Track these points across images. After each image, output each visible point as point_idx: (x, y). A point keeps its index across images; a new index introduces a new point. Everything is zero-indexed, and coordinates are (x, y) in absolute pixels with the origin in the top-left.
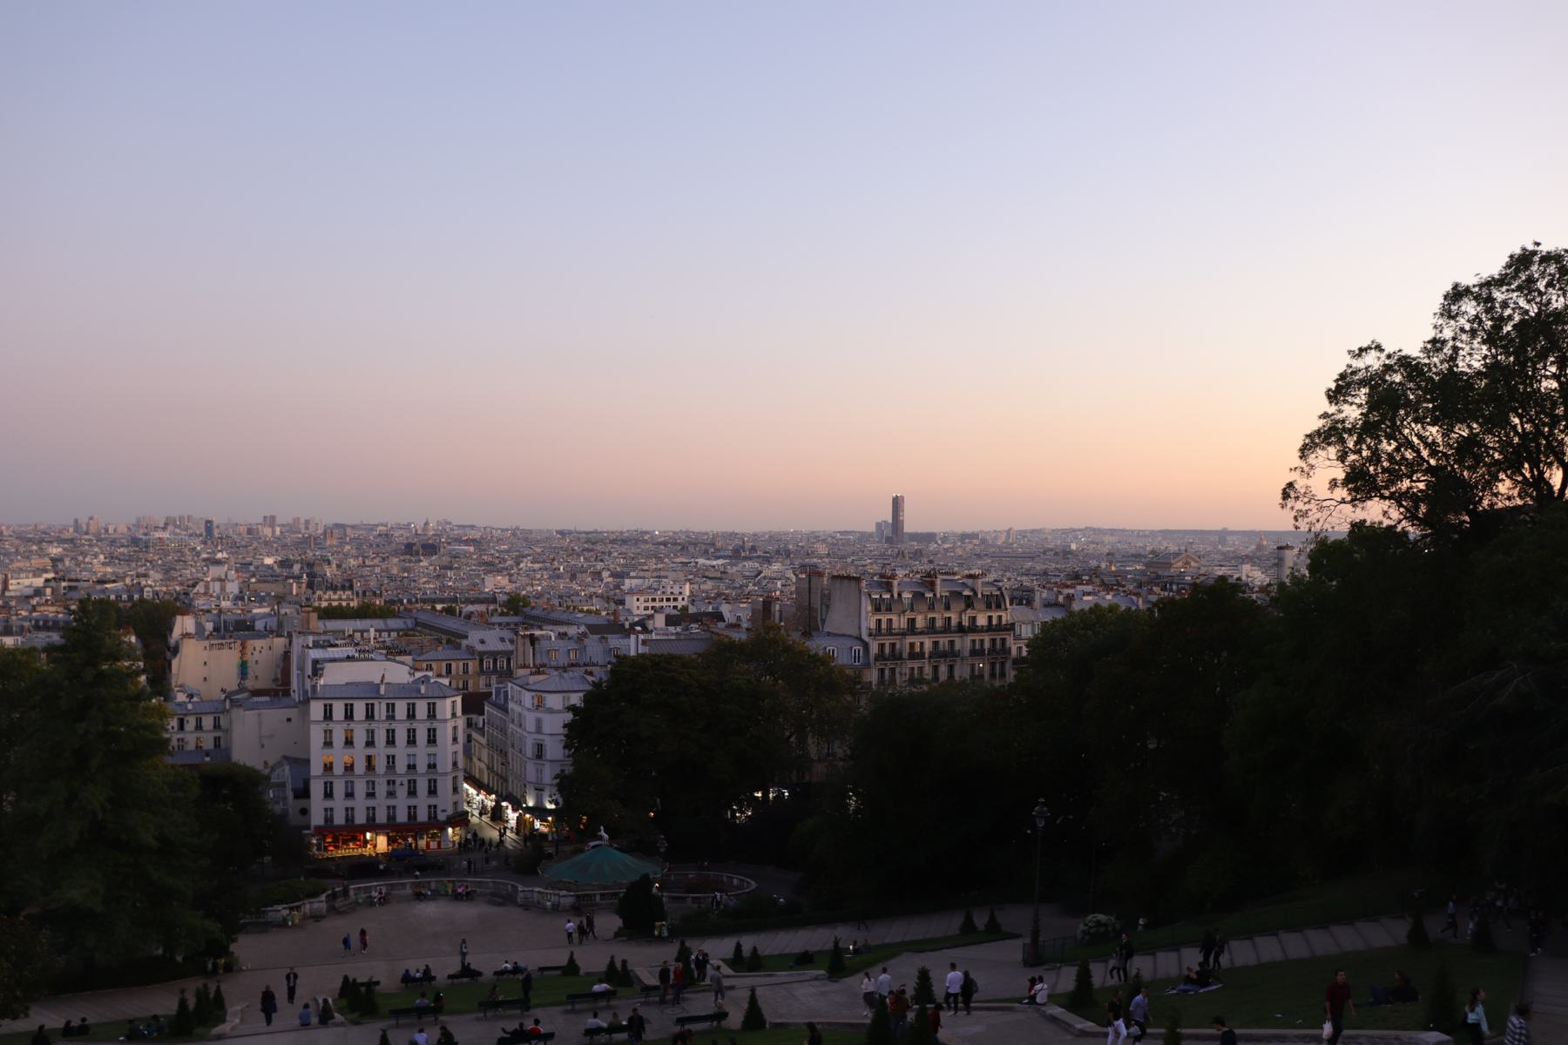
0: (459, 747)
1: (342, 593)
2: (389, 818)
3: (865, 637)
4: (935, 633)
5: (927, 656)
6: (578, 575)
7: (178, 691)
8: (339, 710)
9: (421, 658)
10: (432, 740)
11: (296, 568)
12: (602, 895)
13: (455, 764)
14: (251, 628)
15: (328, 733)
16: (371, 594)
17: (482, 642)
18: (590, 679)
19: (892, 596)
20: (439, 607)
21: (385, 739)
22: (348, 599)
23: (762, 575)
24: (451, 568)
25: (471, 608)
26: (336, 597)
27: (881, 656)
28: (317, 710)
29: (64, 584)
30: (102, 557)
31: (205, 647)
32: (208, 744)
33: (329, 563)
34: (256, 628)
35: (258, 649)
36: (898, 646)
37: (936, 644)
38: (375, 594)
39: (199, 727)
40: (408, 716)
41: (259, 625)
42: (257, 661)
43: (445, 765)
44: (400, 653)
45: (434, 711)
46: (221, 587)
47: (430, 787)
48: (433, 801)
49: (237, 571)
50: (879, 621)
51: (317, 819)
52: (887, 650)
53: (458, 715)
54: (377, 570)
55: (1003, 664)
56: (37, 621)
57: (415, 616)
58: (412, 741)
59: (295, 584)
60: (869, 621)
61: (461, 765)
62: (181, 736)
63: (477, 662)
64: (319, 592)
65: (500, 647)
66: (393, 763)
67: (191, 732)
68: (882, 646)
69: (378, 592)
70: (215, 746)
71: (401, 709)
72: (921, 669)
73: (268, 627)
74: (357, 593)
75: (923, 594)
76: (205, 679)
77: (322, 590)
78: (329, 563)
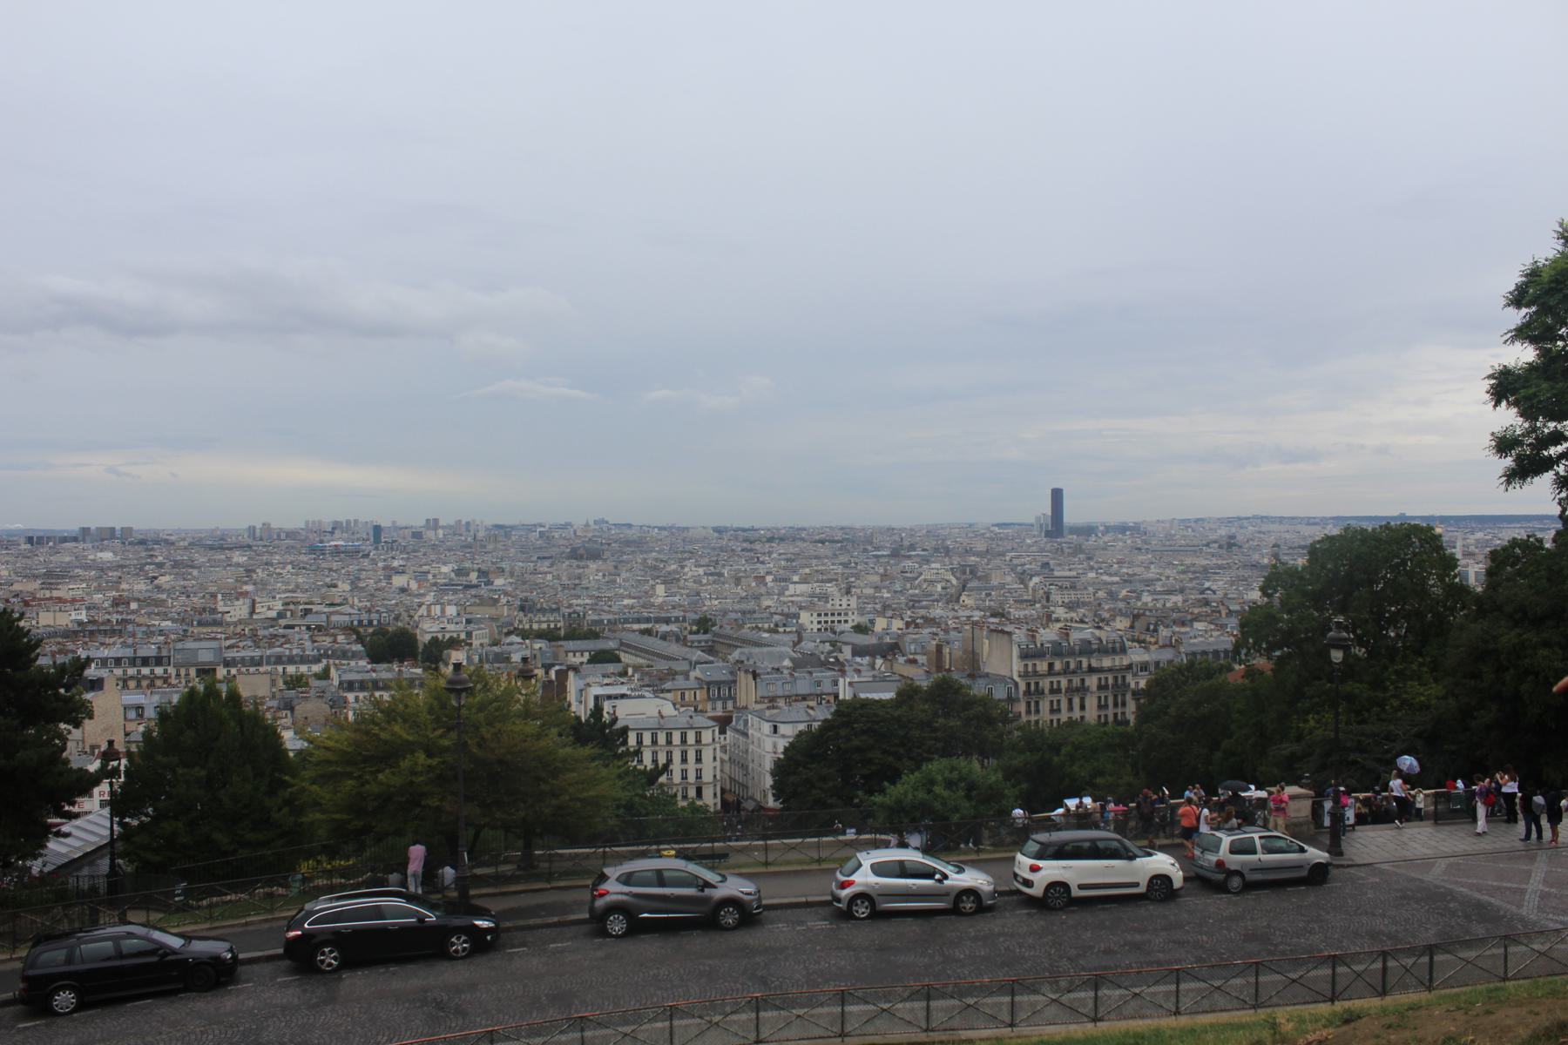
0: (718, 763)
3: (1016, 678)
4: (1070, 673)
5: (1063, 691)
6: (743, 580)
10: (699, 760)
13: (715, 776)
18: (811, 712)
20: (636, 627)
22: (556, 621)
23: (922, 577)
24: (619, 575)
26: (545, 619)
27: (1028, 692)
29: (301, 607)
30: (289, 567)
34: (513, 660)
36: (1041, 684)
37: (1070, 681)
38: (579, 615)
43: (707, 777)
49: (419, 581)
52: (1033, 688)
53: (717, 739)
54: (549, 577)
55: (1124, 695)
58: (684, 760)
60: (1017, 666)
61: (718, 777)
68: (1028, 685)
71: (676, 738)
72: (1059, 701)
78: (503, 571)
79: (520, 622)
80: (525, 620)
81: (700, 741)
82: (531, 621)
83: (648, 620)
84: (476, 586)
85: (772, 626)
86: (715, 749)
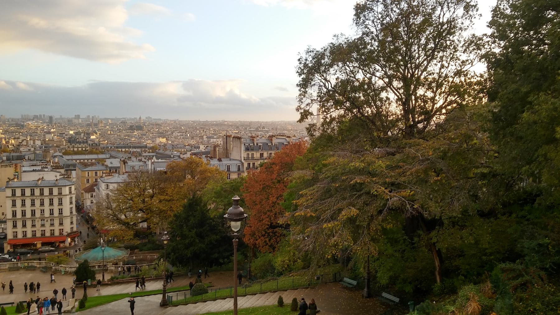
0: (74, 206)
2: (42, 235)
3: (243, 161)
8: (18, 192)
11: (82, 135)
12: (98, 266)
13: (71, 213)
16: (95, 145)
17: (111, 163)
19: (254, 144)
20: (123, 150)
21: (58, 202)
22: (86, 147)
25: (135, 150)
26: (80, 146)
28: (9, 192)
33: (96, 133)
36: (256, 164)
38: (97, 145)
40: (50, 194)
41: (27, 157)
43: (66, 212)
45: (52, 192)
46: (33, 142)
47: (60, 222)
48: (61, 228)
50: (249, 154)
51: (10, 236)
52: (251, 166)
53: (73, 192)
58: (51, 204)
60: (244, 154)
65: (119, 165)
66: (44, 212)
68: (249, 164)
69: (98, 144)
71: (46, 192)
74: (89, 144)
75: (267, 144)
78: (96, 133)
79: (69, 147)
80: (70, 146)
81: (61, 193)
82: (73, 147)
83: (130, 147)
85: (185, 150)
86: (71, 198)
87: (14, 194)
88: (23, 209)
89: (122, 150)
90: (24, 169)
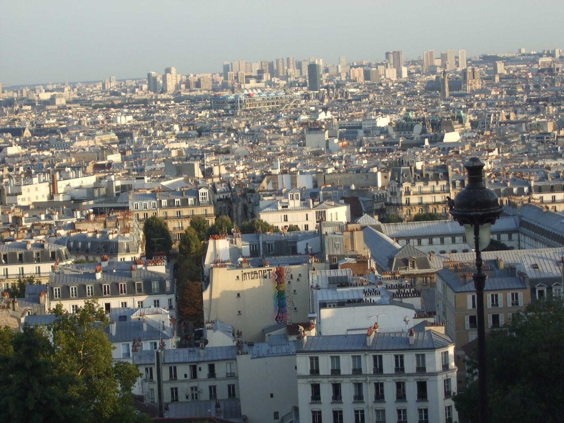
1: (434, 183)
7: (208, 329)
9: (463, 289)
11: (418, 128)
14: (294, 251)
15: (316, 389)
17: (535, 267)
26: (427, 189)
30: (176, 127)
31: (238, 277)
32: (222, 393)
33: (461, 121)
35: (295, 277)
39: (212, 373)
40: (397, 369)
41: (301, 246)
42: (295, 291)
44: (406, 295)
56: (76, 243)
57: (519, 213)
59: (379, 174)
62: (194, 384)
63: (528, 291)
64: (406, 185)
67: (204, 380)
70: (230, 395)
73: (310, 251)
76: (239, 312)
77: (409, 181)
78: (461, 121)
84: (420, 145)
87: (315, 371)
88: (337, 407)
89: (554, 197)
90: (321, 296)
